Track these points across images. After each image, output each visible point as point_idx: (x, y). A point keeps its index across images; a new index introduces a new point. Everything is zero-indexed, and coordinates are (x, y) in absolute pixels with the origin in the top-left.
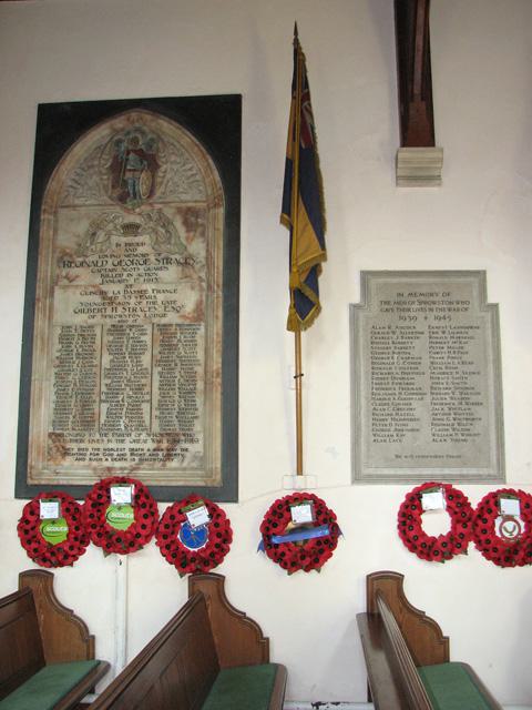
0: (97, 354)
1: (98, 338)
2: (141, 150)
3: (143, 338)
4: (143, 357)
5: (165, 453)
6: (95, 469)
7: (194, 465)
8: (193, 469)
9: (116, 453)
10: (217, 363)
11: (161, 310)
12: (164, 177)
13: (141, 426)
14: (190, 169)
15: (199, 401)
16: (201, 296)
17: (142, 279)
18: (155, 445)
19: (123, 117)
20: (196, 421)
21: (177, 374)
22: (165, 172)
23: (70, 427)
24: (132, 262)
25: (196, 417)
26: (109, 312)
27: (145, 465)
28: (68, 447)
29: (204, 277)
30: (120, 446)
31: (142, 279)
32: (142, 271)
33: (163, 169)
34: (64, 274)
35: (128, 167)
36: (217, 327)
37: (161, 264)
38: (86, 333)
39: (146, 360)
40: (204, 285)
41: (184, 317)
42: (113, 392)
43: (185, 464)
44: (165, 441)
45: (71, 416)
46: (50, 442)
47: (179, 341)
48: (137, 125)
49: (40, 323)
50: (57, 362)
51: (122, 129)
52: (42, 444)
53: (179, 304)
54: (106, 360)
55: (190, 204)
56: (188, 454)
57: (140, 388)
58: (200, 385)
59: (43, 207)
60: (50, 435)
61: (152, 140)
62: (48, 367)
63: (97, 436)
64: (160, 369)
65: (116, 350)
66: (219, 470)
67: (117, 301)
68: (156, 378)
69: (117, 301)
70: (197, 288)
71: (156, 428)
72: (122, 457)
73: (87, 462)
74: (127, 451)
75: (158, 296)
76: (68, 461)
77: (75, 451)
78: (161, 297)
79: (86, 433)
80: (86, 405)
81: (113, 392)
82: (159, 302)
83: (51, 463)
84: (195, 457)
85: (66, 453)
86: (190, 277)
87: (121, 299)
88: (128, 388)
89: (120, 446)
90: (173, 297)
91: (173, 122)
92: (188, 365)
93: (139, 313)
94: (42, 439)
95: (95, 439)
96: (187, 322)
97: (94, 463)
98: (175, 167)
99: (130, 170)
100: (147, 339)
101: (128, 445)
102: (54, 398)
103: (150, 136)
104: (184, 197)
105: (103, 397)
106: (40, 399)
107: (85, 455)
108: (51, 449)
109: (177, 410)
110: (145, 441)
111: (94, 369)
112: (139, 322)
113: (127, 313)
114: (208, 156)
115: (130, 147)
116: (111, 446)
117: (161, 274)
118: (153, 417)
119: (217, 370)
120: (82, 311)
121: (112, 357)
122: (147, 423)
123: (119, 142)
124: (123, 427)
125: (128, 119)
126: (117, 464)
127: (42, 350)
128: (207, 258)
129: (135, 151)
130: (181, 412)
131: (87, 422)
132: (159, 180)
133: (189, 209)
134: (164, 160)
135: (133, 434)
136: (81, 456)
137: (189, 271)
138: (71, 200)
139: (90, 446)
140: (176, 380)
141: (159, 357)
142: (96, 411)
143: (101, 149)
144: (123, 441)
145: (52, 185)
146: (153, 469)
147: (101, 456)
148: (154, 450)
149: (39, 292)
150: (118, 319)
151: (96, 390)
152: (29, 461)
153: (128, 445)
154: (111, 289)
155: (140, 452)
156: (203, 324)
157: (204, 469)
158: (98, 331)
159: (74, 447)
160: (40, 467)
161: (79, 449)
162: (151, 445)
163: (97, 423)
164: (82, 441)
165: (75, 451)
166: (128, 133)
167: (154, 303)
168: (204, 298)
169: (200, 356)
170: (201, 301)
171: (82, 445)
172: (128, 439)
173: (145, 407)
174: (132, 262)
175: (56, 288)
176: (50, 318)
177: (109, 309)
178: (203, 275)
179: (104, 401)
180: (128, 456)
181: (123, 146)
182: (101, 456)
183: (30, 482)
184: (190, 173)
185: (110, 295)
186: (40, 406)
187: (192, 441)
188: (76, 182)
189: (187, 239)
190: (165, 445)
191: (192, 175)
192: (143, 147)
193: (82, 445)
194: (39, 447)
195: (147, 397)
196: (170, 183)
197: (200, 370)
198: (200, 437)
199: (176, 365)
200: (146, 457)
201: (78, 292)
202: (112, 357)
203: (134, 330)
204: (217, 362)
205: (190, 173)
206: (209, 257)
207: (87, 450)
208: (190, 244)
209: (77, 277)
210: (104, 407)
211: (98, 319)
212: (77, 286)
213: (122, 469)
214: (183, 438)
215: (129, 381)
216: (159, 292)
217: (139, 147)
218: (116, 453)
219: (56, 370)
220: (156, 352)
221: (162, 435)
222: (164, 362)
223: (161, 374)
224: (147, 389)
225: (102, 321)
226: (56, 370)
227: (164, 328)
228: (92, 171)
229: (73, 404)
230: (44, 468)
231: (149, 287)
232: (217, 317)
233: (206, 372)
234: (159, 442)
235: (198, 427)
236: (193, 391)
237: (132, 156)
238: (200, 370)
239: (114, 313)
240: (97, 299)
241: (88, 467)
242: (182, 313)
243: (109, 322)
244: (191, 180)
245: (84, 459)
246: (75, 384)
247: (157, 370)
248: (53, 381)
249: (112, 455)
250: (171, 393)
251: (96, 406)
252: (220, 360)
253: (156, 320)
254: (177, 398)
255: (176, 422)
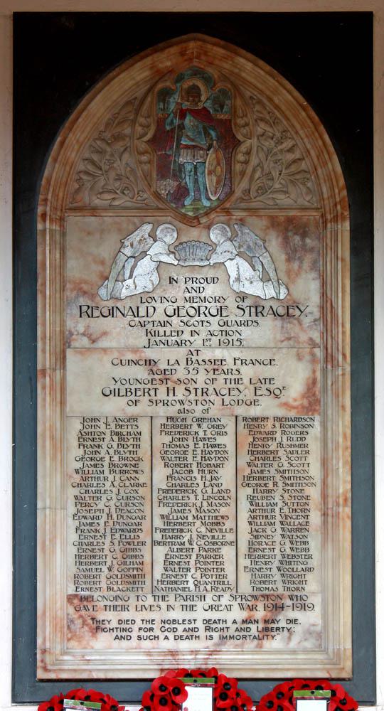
0: (145, 466)
1: (145, 437)
2: (204, 108)
3: (220, 440)
4: (221, 471)
5: (261, 626)
6: (149, 654)
7: (308, 645)
8: (305, 651)
9: (180, 628)
10: (345, 482)
11: (248, 394)
12: (246, 162)
13: (220, 583)
14: (290, 150)
15: (314, 544)
16: (314, 372)
17: (215, 340)
18: (244, 614)
19: (174, 50)
20: (310, 577)
21: (278, 499)
22: (248, 153)
23: (104, 585)
24: (198, 311)
25: (310, 570)
26: (162, 394)
27: (230, 645)
28: (100, 616)
29: (318, 340)
30: (188, 615)
31: (215, 340)
32: (215, 327)
33: (243, 148)
34: (82, 330)
35: (184, 142)
36: (343, 424)
37: (246, 317)
38: (124, 430)
39: (226, 475)
40: (319, 353)
41: (286, 405)
42: (174, 528)
43: (293, 644)
44: (260, 606)
45: (105, 569)
46: (71, 610)
47: (280, 445)
48: (196, 63)
49: (46, 413)
50: (77, 478)
51: (171, 71)
52: (59, 613)
53: (278, 384)
54: (161, 475)
55: (292, 213)
56: (297, 629)
57: (217, 522)
58: (315, 518)
59: (40, 210)
60: (70, 599)
61: (224, 92)
62: (63, 487)
63: (150, 600)
64: (249, 491)
65: (177, 460)
66: (349, 653)
67: (175, 377)
68: (244, 506)
69: (175, 377)
70: (308, 357)
71: (245, 587)
72: (191, 634)
73: (134, 642)
74: (200, 625)
75: (243, 369)
76: (103, 640)
77: (114, 624)
78: (247, 372)
79: (132, 595)
80: (129, 549)
81: (174, 528)
82: (246, 381)
83: (73, 643)
84: (309, 633)
85: (98, 627)
86: (296, 339)
87: (181, 373)
88: (198, 523)
89: (188, 615)
90: (267, 372)
91: (261, 63)
92: (294, 482)
93: (213, 397)
94: (59, 604)
95: (147, 604)
96: (292, 414)
97: (147, 644)
98: (268, 144)
99: (187, 147)
100: (227, 441)
101: (200, 615)
102: (74, 537)
103: (220, 86)
104: (282, 199)
105: (158, 536)
106: (53, 539)
107: (130, 630)
108: (72, 621)
109: (279, 557)
110: (229, 608)
111: (141, 491)
112: (214, 412)
113: (192, 397)
114: (322, 128)
115: (186, 105)
116: (173, 615)
117: (246, 332)
118: (241, 568)
119: (345, 494)
120: (116, 393)
121: (169, 471)
122: (231, 578)
123: (164, 95)
124: (192, 587)
125: (182, 54)
126: (185, 645)
127: (54, 458)
128: (322, 308)
129: (195, 113)
130: (286, 560)
131: (133, 578)
132: (238, 167)
133: (290, 220)
134: (244, 131)
135: (209, 596)
136: (123, 632)
137: (293, 328)
138: (86, 197)
139: (138, 617)
140: (277, 509)
141: (247, 471)
142: (147, 559)
143: (135, 105)
144: (192, 608)
145: (53, 171)
146: (243, 652)
147: (157, 632)
148: (244, 622)
149: (44, 358)
150: (178, 406)
151: (146, 525)
152: (39, 641)
153: (200, 615)
154: (163, 355)
155: (220, 626)
156: (317, 418)
157: (325, 651)
158: (144, 427)
159: (112, 617)
160: (58, 651)
161: (120, 622)
162: (238, 614)
163: (148, 579)
164: (124, 608)
165: (114, 624)
166: (180, 79)
167: (237, 381)
168: (318, 374)
169: (315, 470)
170: (314, 382)
171: (125, 615)
172: (200, 605)
173: (227, 552)
174: (198, 311)
175: (69, 353)
176: (63, 403)
177: (162, 390)
178: (316, 336)
179: (159, 543)
180: (202, 633)
181: (174, 102)
182: (157, 632)
183: (41, 674)
184: (290, 157)
185: (163, 366)
186: (53, 552)
187: (303, 607)
188: (93, 163)
189: (288, 273)
190: (260, 614)
191: (294, 161)
192: (208, 105)
193: (125, 615)
194: (55, 618)
195: (230, 537)
196: (258, 175)
197: (314, 493)
198: (316, 600)
199: (275, 484)
200: (232, 632)
201: (107, 359)
202: (169, 471)
203: (204, 425)
204: (342, 482)
205: (290, 157)
206: (326, 306)
207: (133, 622)
208: (294, 282)
209: (105, 334)
210: (160, 552)
211: (144, 407)
212: (105, 350)
213: (192, 652)
214: (289, 602)
215: (199, 510)
216: (243, 362)
217: (200, 106)
218: (180, 628)
219: (76, 491)
220: (243, 462)
221: (255, 598)
222: (256, 480)
223: (251, 500)
224: (229, 524)
225: (151, 410)
226: (76, 491)
227: (254, 423)
228: (119, 146)
229: (107, 547)
230: (65, 653)
231: (228, 354)
232: (343, 407)
233: (324, 496)
234: (252, 608)
235: (312, 585)
236: (304, 527)
237: (188, 121)
238: (314, 493)
239: (171, 398)
240: (141, 373)
241: (137, 650)
242: (283, 399)
243: (162, 411)
244: (293, 168)
245: (128, 638)
246: (109, 515)
247: (245, 492)
248: (72, 509)
249: (174, 630)
250: (268, 529)
251: (146, 551)
252: (349, 478)
253: (241, 411)
254: (278, 538)
255: (278, 577)
